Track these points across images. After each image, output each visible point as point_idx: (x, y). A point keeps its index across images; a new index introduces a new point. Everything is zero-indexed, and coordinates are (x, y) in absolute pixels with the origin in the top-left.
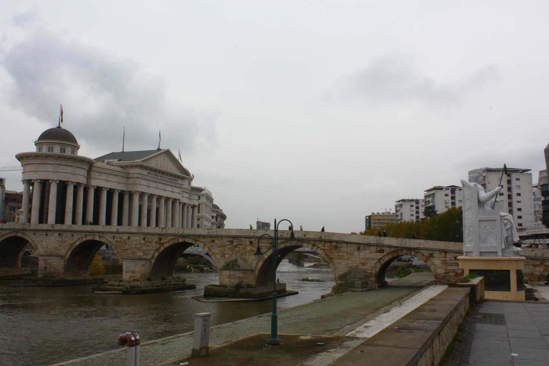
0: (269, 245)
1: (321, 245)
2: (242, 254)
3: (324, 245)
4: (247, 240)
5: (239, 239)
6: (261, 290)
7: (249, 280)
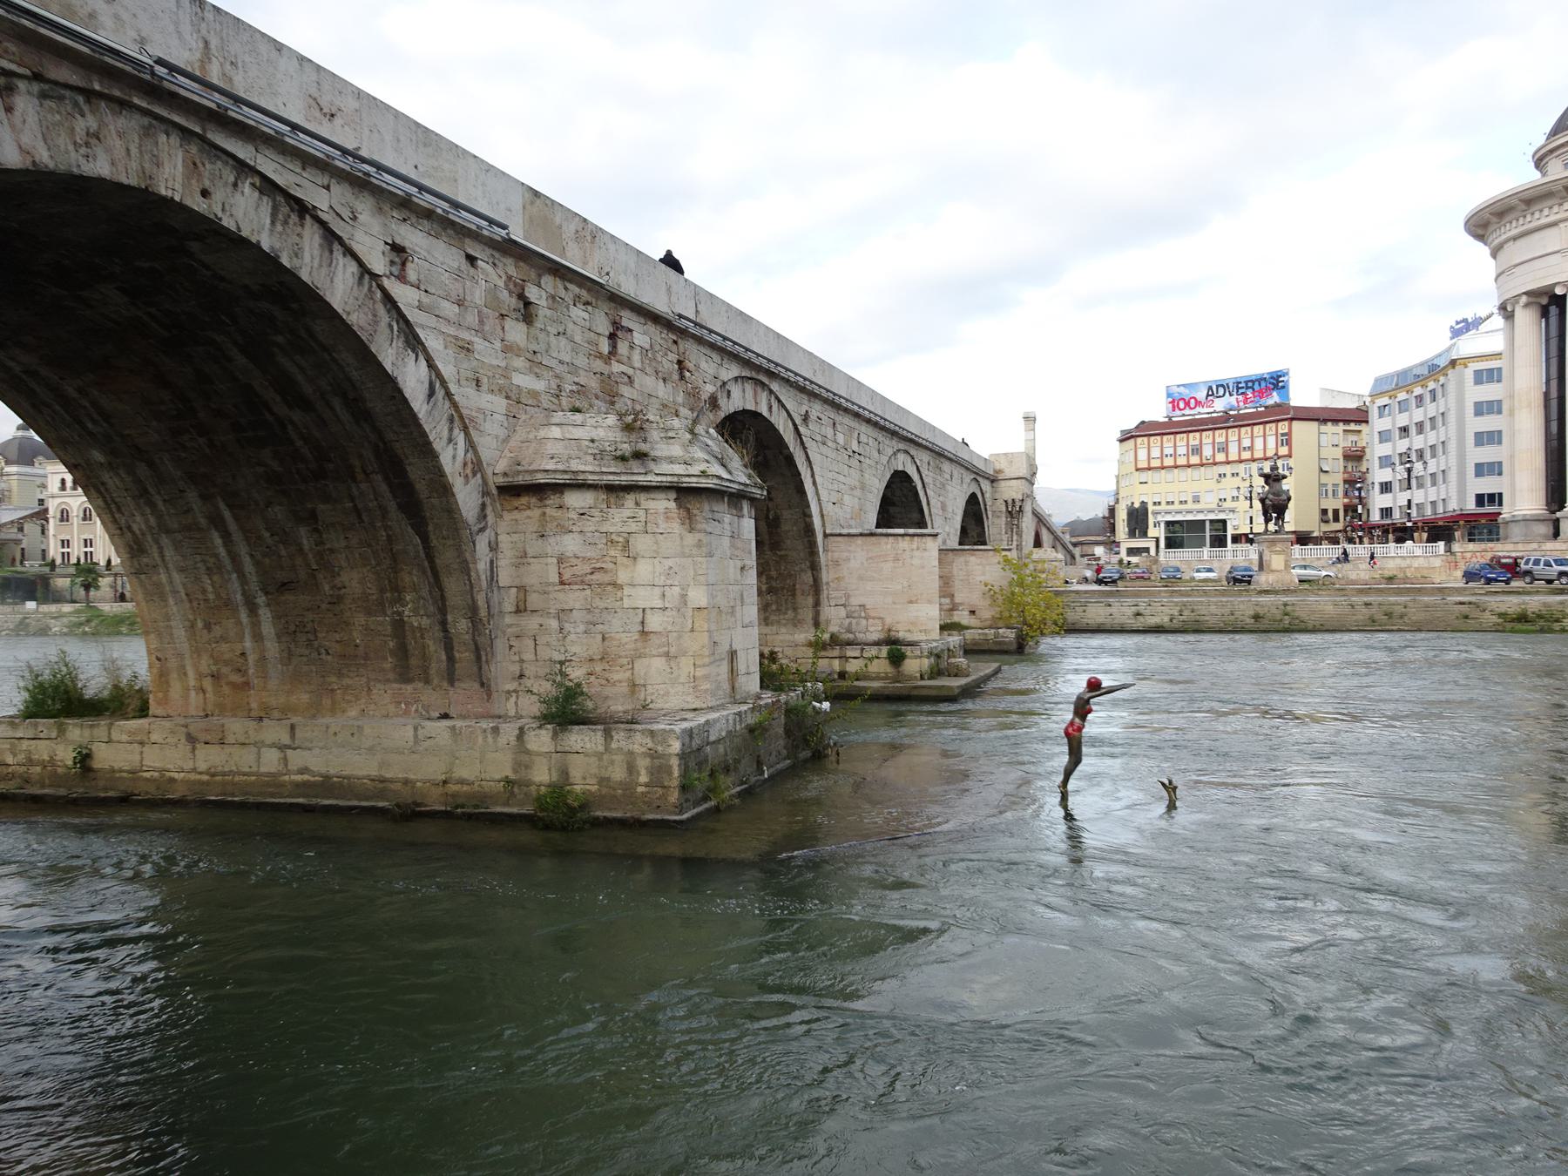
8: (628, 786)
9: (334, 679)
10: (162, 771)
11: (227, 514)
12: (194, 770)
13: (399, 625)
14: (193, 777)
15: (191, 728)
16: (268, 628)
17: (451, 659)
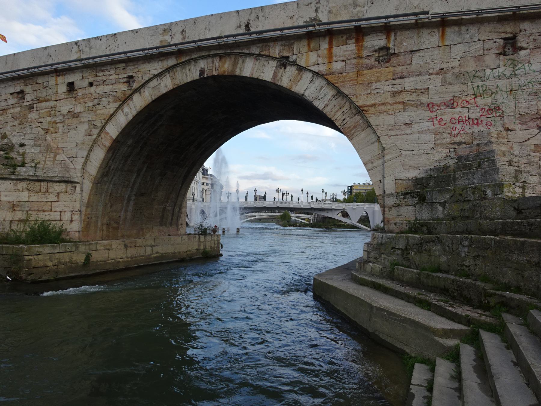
0: (124, 87)
1: (313, 57)
2: (46, 131)
3: (330, 56)
4: (60, 79)
5: (40, 80)
6: (112, 251)
7: (55, 216)
8: (214, 247)
9: (144, 225)
10: (115, 259)
11: (145, 169)
12: (127, 257)
13: (164, 209)
14: (126, 260)
15: (126, 242)
16: (131, 208)
17: (172, 219)
